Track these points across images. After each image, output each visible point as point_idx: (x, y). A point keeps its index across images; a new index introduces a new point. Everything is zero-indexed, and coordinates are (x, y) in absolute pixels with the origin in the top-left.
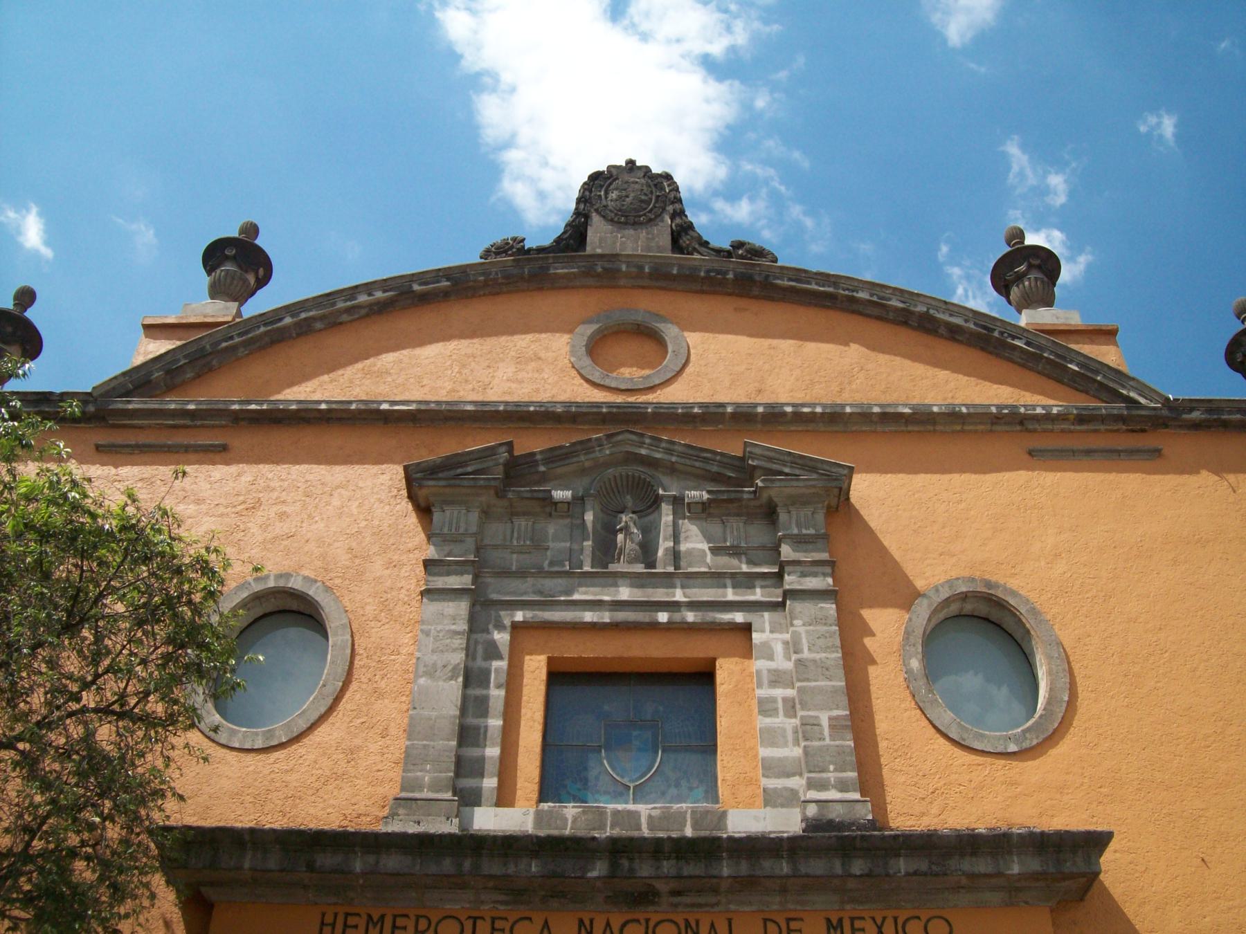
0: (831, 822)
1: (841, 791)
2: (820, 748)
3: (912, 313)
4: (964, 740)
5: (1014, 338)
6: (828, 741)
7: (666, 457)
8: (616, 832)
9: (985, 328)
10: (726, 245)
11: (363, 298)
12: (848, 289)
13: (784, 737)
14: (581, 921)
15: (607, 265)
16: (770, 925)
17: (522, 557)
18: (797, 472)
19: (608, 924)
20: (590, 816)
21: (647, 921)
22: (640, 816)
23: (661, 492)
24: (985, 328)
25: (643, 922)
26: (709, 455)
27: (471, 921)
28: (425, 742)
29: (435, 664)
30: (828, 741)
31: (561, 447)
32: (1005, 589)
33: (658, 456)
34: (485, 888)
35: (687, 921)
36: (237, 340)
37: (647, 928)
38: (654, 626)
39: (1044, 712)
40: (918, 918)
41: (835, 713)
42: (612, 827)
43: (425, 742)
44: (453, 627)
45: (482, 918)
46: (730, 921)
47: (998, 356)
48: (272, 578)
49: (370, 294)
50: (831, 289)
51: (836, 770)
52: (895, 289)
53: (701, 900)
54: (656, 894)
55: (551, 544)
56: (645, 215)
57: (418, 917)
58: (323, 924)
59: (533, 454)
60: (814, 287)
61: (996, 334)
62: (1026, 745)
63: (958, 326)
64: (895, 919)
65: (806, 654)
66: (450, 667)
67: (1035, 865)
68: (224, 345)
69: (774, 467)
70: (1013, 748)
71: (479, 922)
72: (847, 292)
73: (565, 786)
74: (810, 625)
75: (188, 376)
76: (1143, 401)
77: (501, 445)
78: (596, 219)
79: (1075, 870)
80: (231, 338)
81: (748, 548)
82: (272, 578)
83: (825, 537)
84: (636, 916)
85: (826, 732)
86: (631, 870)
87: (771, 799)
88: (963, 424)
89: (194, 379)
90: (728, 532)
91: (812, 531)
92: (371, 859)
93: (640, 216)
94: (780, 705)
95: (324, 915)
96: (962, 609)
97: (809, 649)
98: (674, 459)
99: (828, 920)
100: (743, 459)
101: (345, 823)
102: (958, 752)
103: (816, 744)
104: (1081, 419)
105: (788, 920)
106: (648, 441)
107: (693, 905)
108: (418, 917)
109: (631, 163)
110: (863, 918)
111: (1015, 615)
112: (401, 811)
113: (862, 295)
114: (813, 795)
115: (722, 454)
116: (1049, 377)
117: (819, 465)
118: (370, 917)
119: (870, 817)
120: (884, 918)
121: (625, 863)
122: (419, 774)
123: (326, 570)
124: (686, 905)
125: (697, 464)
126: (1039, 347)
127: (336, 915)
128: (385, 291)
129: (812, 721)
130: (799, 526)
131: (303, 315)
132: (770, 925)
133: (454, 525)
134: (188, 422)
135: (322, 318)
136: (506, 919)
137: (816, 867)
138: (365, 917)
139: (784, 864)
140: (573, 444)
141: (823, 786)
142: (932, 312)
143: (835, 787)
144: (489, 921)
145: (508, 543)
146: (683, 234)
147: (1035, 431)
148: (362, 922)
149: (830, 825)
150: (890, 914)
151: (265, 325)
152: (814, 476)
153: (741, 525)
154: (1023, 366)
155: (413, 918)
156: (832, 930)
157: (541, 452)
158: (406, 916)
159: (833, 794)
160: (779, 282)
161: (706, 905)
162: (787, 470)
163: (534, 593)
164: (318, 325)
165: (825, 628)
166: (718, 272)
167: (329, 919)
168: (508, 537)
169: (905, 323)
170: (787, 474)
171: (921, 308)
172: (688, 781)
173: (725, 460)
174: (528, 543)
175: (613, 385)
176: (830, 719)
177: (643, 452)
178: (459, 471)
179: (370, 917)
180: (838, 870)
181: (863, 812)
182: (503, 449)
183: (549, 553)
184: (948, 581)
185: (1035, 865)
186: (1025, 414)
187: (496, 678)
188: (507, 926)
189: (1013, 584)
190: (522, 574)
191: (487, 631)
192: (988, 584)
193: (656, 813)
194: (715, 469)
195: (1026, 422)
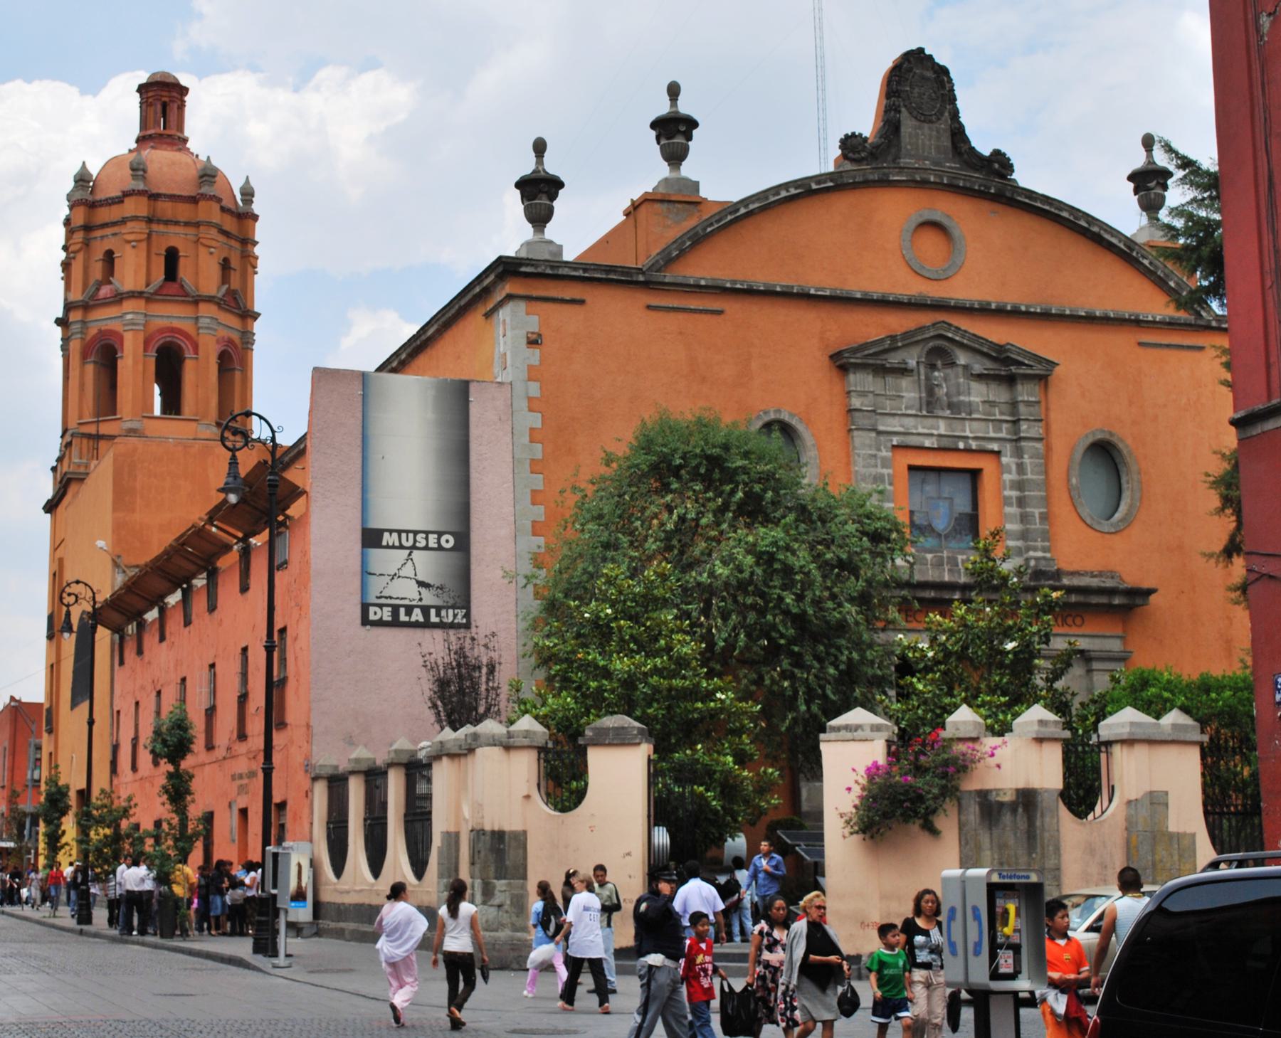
2: (1034, 529)
6: (1038, 526)
9: (1129, 248)
11: (784, 194)
15: (925, 176)
30: (1038, 526)
33: (957, 338)
38: (957, 450)
47: (1132, 265)
49: (788, 191)
50: (1047, 207)
55: (904, 394)
60: (1039, 205)
61: (1134, 254)
65: (1030, 476)
68: (709, 230)
69: (1020, 359)
70: (1113, 530)
85: (1038, 521)
94: (1014, 501)
102: (1090, 530)
103: (1033, 527)
104: (1169, 324)
113: (1065, 214)
116: (1156, 284)
126: (1156, 267)
141: (1035, 549)
142: (1102, 232)
151: (730, 213)
154: (1144, 274)
160: (1019, 198)
162: (1026, 362)
166: (985, 186)
171: (1095, 229)
175: (927, 275)
177: (950, 335)
183: (904, 400)
192: (1111, 434)
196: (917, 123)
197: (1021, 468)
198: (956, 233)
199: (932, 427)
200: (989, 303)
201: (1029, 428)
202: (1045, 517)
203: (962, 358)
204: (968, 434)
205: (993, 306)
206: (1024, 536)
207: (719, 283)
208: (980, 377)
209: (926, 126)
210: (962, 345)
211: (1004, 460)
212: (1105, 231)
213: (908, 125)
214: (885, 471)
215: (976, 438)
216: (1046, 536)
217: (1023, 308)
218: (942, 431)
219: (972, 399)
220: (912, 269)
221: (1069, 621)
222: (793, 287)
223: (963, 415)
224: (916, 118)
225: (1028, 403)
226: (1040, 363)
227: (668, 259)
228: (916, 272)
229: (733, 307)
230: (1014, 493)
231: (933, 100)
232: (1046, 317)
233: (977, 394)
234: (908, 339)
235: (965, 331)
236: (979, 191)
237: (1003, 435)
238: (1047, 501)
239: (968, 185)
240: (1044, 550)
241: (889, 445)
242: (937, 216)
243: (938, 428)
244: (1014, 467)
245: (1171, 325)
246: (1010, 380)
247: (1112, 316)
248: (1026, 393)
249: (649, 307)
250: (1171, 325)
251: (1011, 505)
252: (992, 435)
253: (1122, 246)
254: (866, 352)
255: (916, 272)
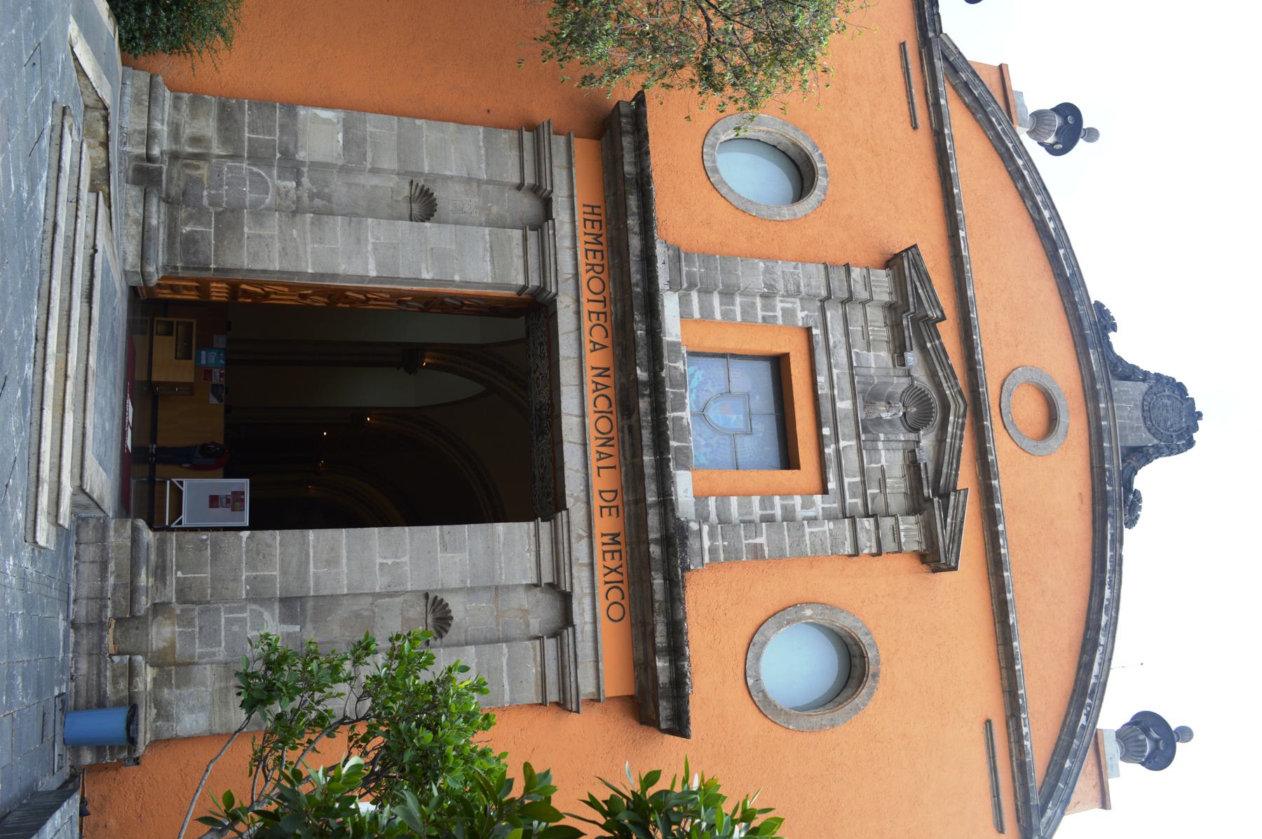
0: (687, 538)
1: (709, 549)
2: (739, 536)
3: (1098, 633)
4: (754, 645)
5: (1087, 715)
7: (949, 435)
8: (670, 396)
9: (1093, 691)
10: (1136, 486)
11: (1046, 214)
12: (1111, 581)
13: (746, 514)
14: (607, 369)
15: (1102, 394)
16: (614, 494)
17: (860, 333)
18: (948, 528)
19: (607, 387)
20: (679, 378)
21: (611, 412)
22: (682, 411)
23: (922, 432)
24: (1093, 691)
25: (610, 410)
26: (954, 466)
27: (602, 299)
28: (719, 268)
29: (774, 273)
31: (947, 357)
32: (873, 688)
33: (950, 429)
34: (624, 306)
35: (613, 438)
36: (999, 128)
37: (606, 413)
39: (779, 707)
40: (623, 598)
41: (766, 548)
42: (673, 393)
43: (719, 268)
44: (802, 284)
45: (605, 306)
46: (614, 467)
48: (823, 165)
49: (1050, 219)
50: (1108, 567)
51: (724, 546)
52: (1116, 618)
53: (627, 447)
54: (629, 417)
55: (872, 353)
56: (1153, 425)
57: (603, 266)
58: (593, 207)
59: (939, 338)
60: (1109, 554)
61: (1088, 701)
62: (753, 693)
63: (1091, 670)
64: (621, 582)
65: (807, 530)
66: (773, 283)
67: (663, 679)
68: (994, 120)
69: (950, 511)
70: (750, 681)
71: (603, 304)
72: (1107, 580)
73: (700, 369)
74: (830, 534)
75: (966, 99)
76: (1044, 820)
77: (942, 312)
78: (1144, 387)
79: (661, 709)
80: (1000, 124)
81: (885, 495)
82: (823, 165)
83: (900, 551)
84: (613, 405)
85: (751, 541)
86: (644, 395)
87: (700, 498)
88: (1006, 668)
89: (965, 103)
90: (896, 480)
91: (903, 540)
92: (637, 229)
93: (1151, 421)
94: (769, 512)
95: (599, 207)
96: (855, 656)
97: (812, 533)
98: (948, 440)
99: (618, 535)
100: (955, 490)
101: (660, 221)
102: (745, 642)
105: (617, 507)
106: (960, 420)
107: (623, 442)
108: (603, 266)
109: (1200, 415)
110: (621, 559)
111: (854, 694)
112: (671, 252)
113: (1107, 593)
114: (706, 528)
115: (957, 475)
116: (1057, 745)
117: (956, 545)
118: (601, 235)
119: (692, 567)
120: (622, 574)
121: (647, 392)
122: (698, 264)
123: (834, 201)
124: (623, 438)
125: (946, 457)
126: (1082, 737)
127: (600, 215)
128: (1054, 229)
129: (758, 531)
130: (906, 530)
131: (1025, 173)
132: (614, 494)
133: (877, 284)
134: (931, 101)
135: (1027, 187)
136: (606, 321)
137: (653, 520)
138: (600, 233)
139: (654, 499)
140: (950, 367)
141: (712, 536)
142: (1101, 648)
143: (712, 544)
144: (604, 310)
145: (869, 324)
146: (1139, 456)
147: (1008, 727)
148: (595, 231)
149: (684, 538)
150: (625, 578)
152: (947, 541)
153: (903, 490)
155: (601, 263)
156: (611, 537)
157: (941, 344)
158: (603, 259)
159: (707, 543)
160: (1109, 526)
161: (624, 451)
162: (949, 520)
163: (834, 342)
164: (1020, 185)
165: (829, 545)
166: (1111, 477)
167: (596, 210)
168: (873, 324)
169: (1087, 628)
170: (946, 521)
171: (1102, 640)
172: (710, 453)
173: (952, 478)
174: (871, 337)
176: (761, 545)
177: (951, 418)
178: (918, 284)
179: (601, 235)
180: (652, 536)
181: (695, 562)
182: (939, 314)
184: (874, 642)
185: (663, 679)
186: (1020, 718)
187: (769, 316)
188: (601, 322)
189: (879, 694)
190: (847, 334)
191: (803, 310)
192: (875, 676)
193: (685, 421)
194: (944, 470)
195: (1014, 719)
196: (1139, 403)
197: (812, 520)
198: (1053, 442)
199: (841, 390)
200: (997, 477)
201: (868, 531)
202: (756, 552)
203: (927, 441)
204: (842, 444)
205: (995, 483)
206: (724, 520)
207: (946, 121)
208: (913, 465)
209: (1138, 413)
210: (940, 441)
211: (818, 498)
212: (1104, 653)
213: (1136, 390)
214: (779, 313)
215: (838, 451)
216: (733, 555)
217: (1001, 527)
218: (839, 405)
219: (883, 452)
220: (1004, 380)
221: (615, 595)
222: (961, 209)
223: (863, 437)
224: (1144, 400)
225: (896, 531)
226: (952, 540)
227: (955, 64)
228: (1002, 386)
229: (922, 140)
230: (778, 512)
231: (1165, 422)
232: (995, 565)
233: (890, 460)
234: (934, 359)
235: (961, 438)
236: (1103, 470)
237: (849, 500)
238: (779, 556)
239: (1107, 454)
240: (713, 551)
241: (811, 324)
242: (1063, 418)
243: (842, 400)
244: (811, 513)
245: (1021, 768)
246: (917, 505)
247: (1017, 667)
248: (910, 529)
249: (904, 44)
250: (1021, 768)
251: (763, 507)
252: (846, 480)
253: (1093, 681)
254: (918, 284)
255: (1002, 386)
